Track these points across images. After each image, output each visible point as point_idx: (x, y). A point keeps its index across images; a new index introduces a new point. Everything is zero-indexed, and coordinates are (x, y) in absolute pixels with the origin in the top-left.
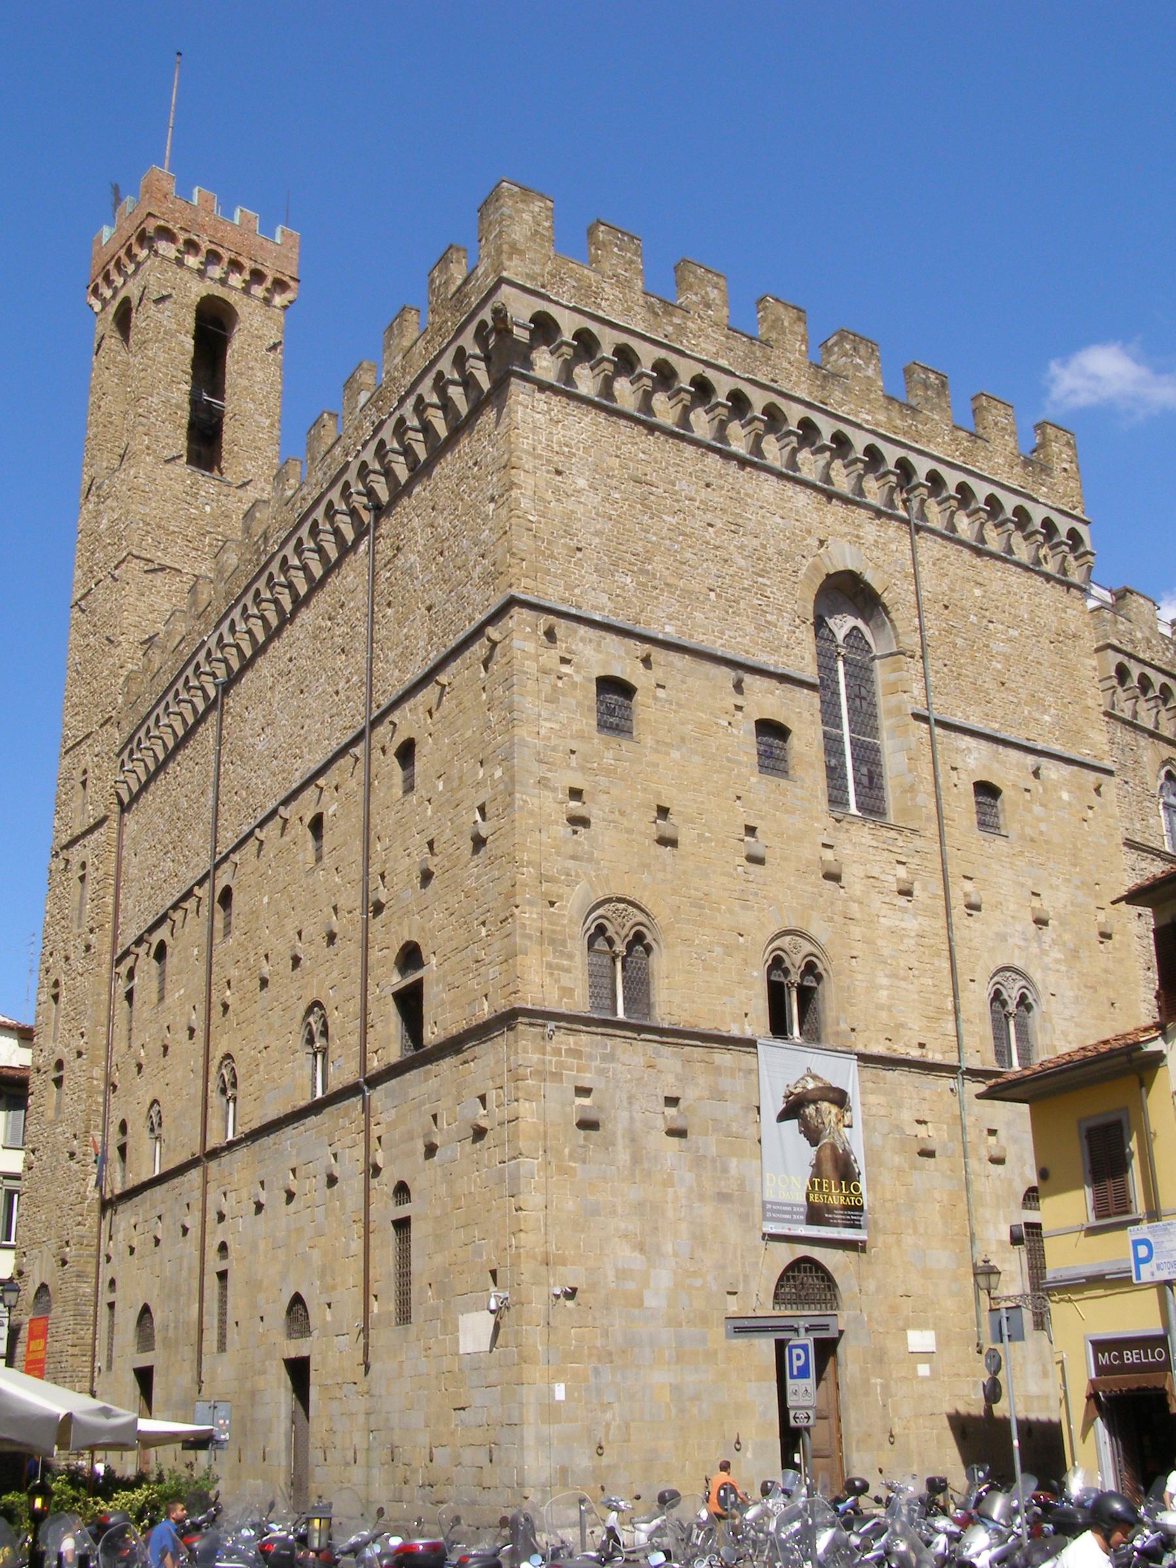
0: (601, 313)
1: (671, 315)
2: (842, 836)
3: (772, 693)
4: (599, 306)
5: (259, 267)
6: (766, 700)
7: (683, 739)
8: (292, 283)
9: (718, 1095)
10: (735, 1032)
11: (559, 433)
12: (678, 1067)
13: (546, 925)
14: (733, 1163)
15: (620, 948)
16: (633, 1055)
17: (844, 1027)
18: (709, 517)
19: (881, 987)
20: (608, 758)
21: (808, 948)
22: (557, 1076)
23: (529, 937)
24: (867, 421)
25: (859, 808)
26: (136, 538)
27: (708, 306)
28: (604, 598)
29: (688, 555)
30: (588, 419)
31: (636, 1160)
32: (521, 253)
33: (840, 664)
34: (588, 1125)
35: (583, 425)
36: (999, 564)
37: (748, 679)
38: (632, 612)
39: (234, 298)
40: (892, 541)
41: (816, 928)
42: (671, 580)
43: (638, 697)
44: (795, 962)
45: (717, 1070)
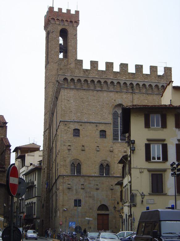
0: (75, 75)
1: (87, 71)
2: (115, 145)
3: (103, 126)
4: (75, 74)
5: (71, 20)
6: (102, 128)
7: (87, 136)
8: (78, 22)
9: (90, 183)
10: (93, 175)
11: (68, 95)
12: (83, 180)
13: (64, 164)
14: (92, 193)
15: (76, 166)
16: (76, 180)
17: (112, 173)
18: (94, 101)
19: (120, 166)
20: (75, 140)
21: (107, 162)
22: (65, 183)
23: (62, 166)
24: (124, 79)
25: (121, 139)
26: (51, 79)
27: (94, 67)
28: (75, 118)
29: (90, 108)
30: (73, 91)
31: (76, 192)
32: (62, 69)
33: (119, 118)
34: (69, 189)
35: (72, 93)
36: (152, 95)
37: (98, 124)
38: (79, 119)
39: (67, 28)
40: (129, 97)
41: (109, 159)
42: (86, 113)
43: (80, 131)
44: (105, 165)
45: (90, 180)
